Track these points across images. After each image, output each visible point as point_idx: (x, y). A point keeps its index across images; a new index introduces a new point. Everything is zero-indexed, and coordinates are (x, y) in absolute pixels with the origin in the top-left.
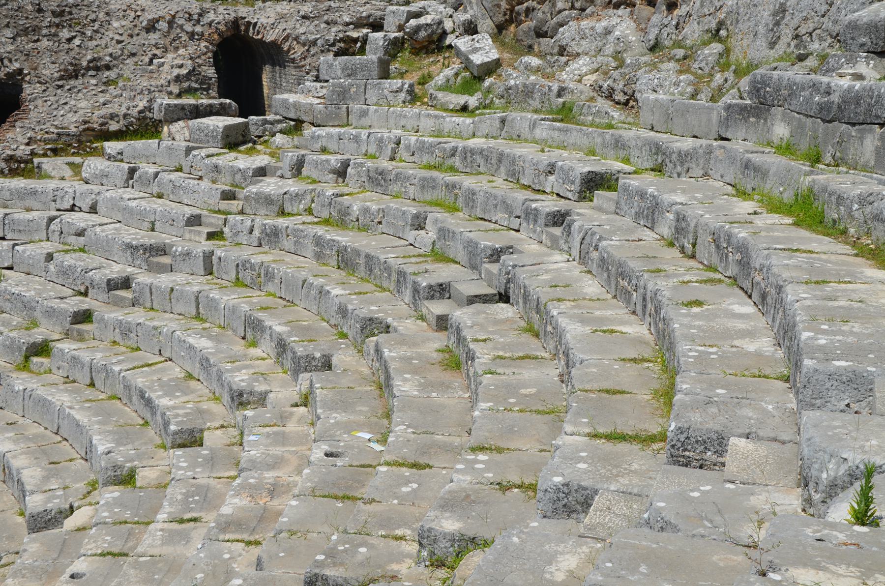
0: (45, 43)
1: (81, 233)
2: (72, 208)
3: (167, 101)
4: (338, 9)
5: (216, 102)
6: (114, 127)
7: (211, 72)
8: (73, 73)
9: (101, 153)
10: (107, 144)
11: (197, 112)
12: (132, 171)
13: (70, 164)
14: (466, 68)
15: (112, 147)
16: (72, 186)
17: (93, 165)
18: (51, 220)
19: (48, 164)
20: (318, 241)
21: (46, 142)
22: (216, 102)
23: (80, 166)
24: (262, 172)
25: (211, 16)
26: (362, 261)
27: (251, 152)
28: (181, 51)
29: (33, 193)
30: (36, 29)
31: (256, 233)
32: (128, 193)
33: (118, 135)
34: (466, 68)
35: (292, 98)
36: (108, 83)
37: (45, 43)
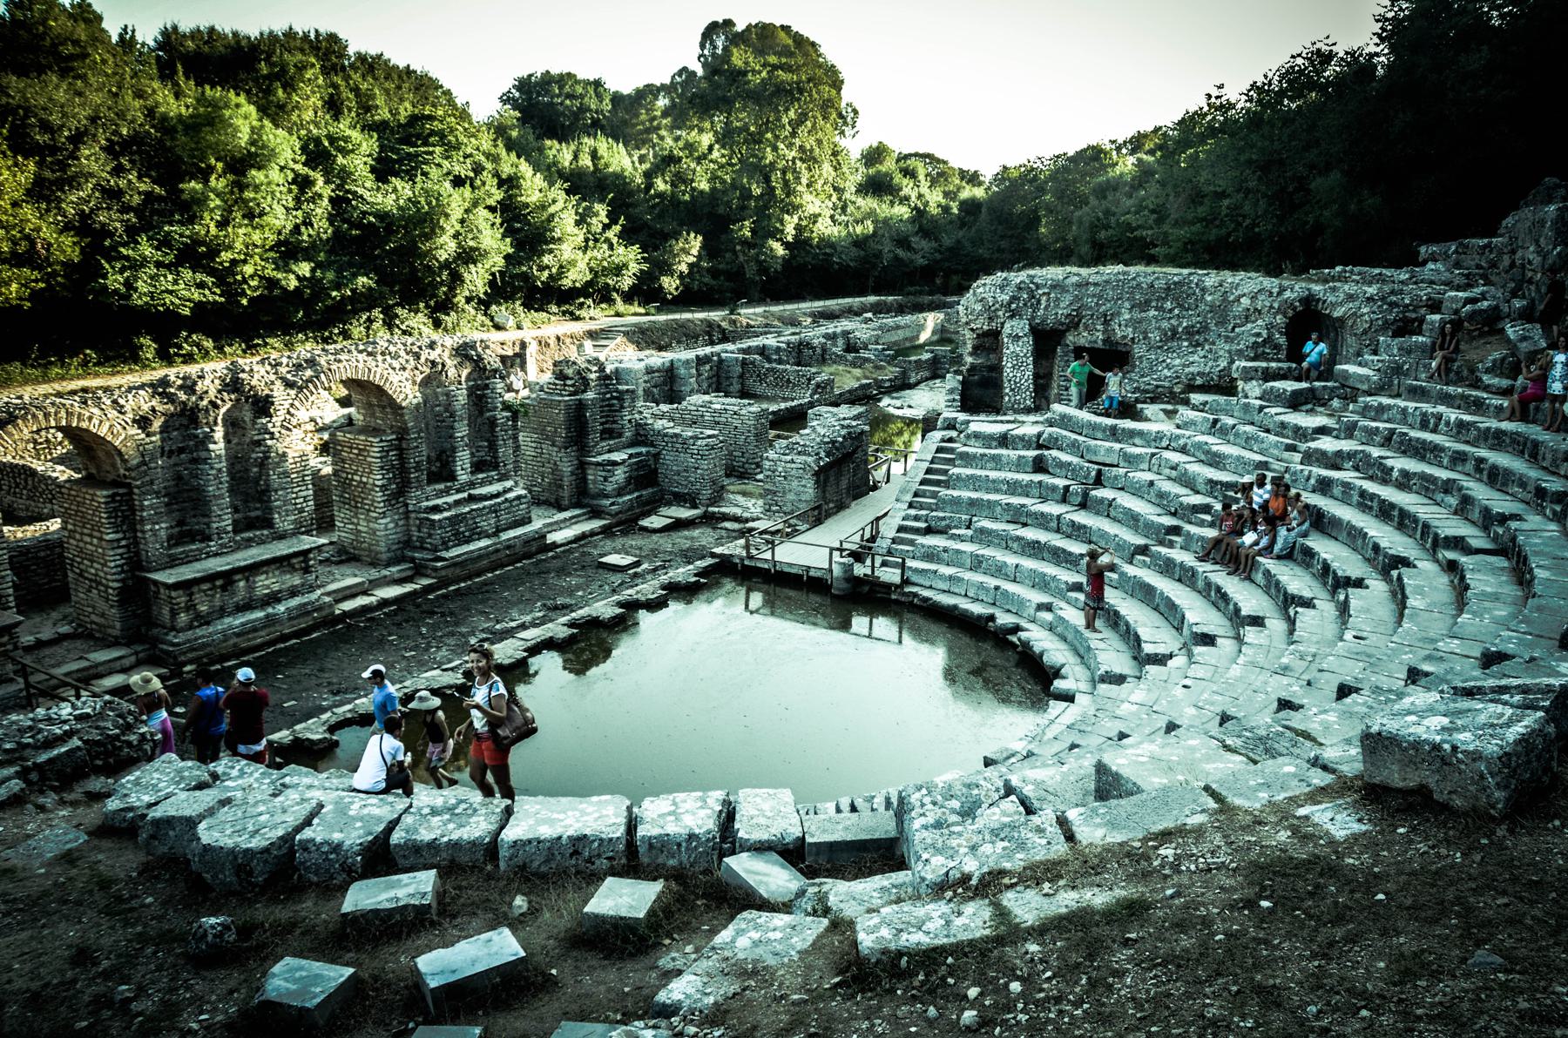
0: (1153, 313)
1: (1174, 468)
2: (1167, 448)
3: (1244, 364)
4: (1401, 292)
5: (1285, 365)
6: (1199, 381)
7: (1282, 340)
8: (1174, 335)
9: (1186, 402)
10: (1192, 396)
11: (1268, 376)
12: (1216, 421)
13: (1164, 411)
14: (1513, 355)
15: (1196, 398)
16: (1167, 427)
17: (1186, 413)
18: (1153, 455)
19: (1151, 410)
20: (1363, 493)
21: (1147, 391)
22: (1285, 365)
23: (1176, 412)
24: (1322, 431)
25: (1288, 294)
26: (1396, 513)
27: (1310, 412)
28: (1260, 322)
29: (1141, 434)
30: (1147, 302)
31: (1312, 481)
32: (1210, 439)
33: (1204, 389)
34: (1513, 355)
35: (1351, 368)
36: (1198, 345)
37: (1153, 313)
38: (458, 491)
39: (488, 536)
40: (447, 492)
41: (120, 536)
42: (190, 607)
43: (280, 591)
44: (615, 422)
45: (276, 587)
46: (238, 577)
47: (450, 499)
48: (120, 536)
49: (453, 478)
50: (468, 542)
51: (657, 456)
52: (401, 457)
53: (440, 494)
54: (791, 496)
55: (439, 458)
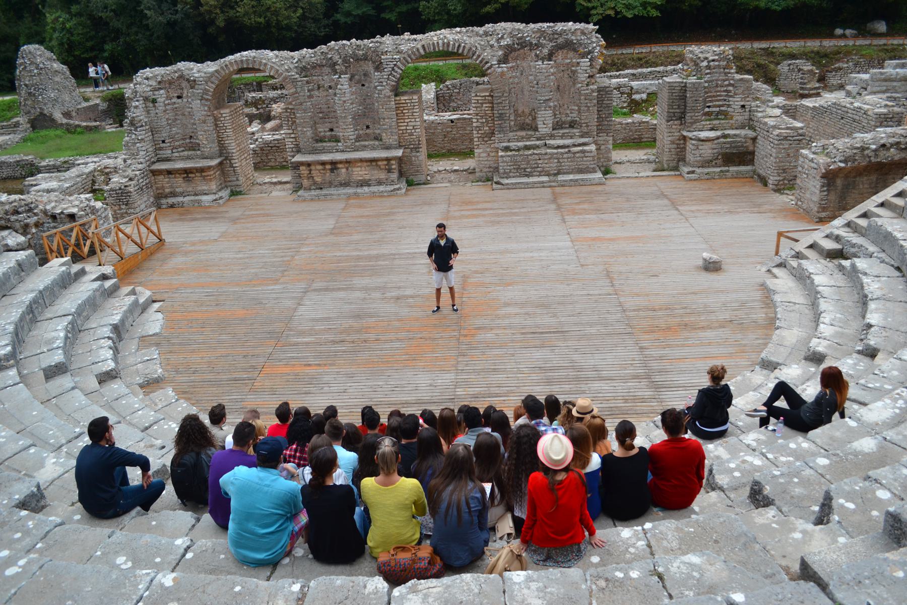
38: (538, 139)
39: (548, 175)
40: (528, 138)
41: (291, 131)
42: (310, 177)
43: (370, 180)
44: (729, 106)
45: (367, 177)
46: (340, 166)
47: (520, 144)
48: (291, 131)
50: (528, 176)
51: (754, 139)
52: (492, 108)
53: (522, 139)
54: (808, 195)
55: (530, 114)
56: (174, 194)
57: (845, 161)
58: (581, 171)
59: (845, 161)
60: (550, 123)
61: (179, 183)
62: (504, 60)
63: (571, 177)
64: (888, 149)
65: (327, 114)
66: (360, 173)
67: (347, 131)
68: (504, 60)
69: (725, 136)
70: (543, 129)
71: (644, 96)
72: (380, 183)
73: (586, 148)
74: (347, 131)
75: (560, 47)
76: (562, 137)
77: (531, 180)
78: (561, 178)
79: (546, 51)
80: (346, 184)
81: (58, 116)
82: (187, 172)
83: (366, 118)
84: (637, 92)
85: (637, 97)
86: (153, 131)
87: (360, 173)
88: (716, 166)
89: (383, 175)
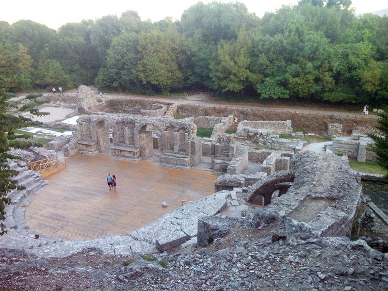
39: (174, 164)
40: (172, 153)
49: (174, 150)
53: (170, 152)
56: (83, 150)
57: (220, 183)
58: (183, 165)
59: (220, 183)
60: (178, 149)
61: (85, 148)
62: (166, 130)
63: (180, 166)
64: (232, 182)
65: (123, 136)
66: (127, 154)
67: (127, 142)
68: (166, 130)
69: (224, 163)
70: (175, 151)
71: (253, 134)
72: (132, 158)
73: (184, 159)
74: (127, 142)
75: (181, 129)
76: (181, 154)
77: (170, 165)
78: (177, 166)
79: (177, 129)
80: (124, 156)
81: (86, 108)
82: (87, 145)
83: (132, 138)
84: (251, 132)
85: (250, 134)
86: (81, 132)
87: (127, 154)
88: (220, 171)
89: (132, 156)
